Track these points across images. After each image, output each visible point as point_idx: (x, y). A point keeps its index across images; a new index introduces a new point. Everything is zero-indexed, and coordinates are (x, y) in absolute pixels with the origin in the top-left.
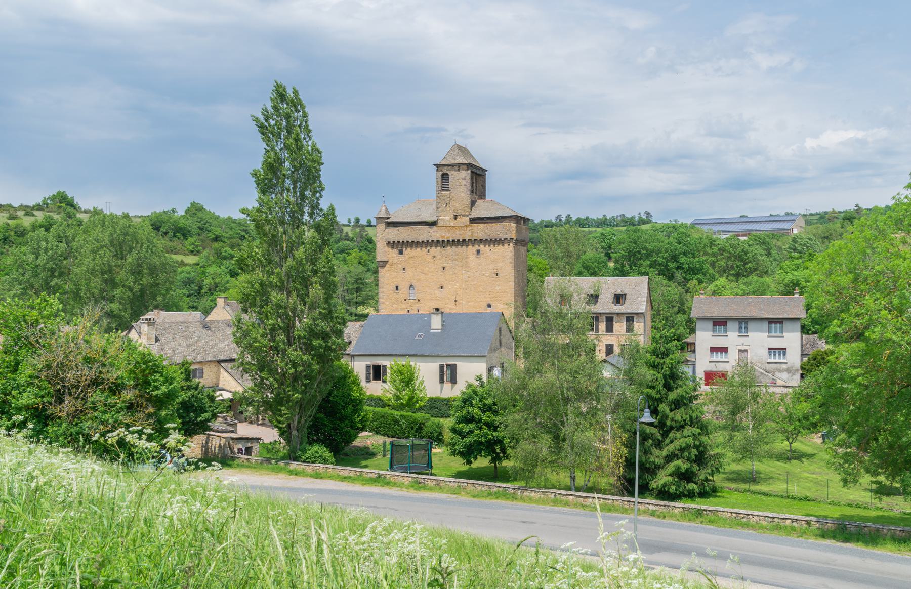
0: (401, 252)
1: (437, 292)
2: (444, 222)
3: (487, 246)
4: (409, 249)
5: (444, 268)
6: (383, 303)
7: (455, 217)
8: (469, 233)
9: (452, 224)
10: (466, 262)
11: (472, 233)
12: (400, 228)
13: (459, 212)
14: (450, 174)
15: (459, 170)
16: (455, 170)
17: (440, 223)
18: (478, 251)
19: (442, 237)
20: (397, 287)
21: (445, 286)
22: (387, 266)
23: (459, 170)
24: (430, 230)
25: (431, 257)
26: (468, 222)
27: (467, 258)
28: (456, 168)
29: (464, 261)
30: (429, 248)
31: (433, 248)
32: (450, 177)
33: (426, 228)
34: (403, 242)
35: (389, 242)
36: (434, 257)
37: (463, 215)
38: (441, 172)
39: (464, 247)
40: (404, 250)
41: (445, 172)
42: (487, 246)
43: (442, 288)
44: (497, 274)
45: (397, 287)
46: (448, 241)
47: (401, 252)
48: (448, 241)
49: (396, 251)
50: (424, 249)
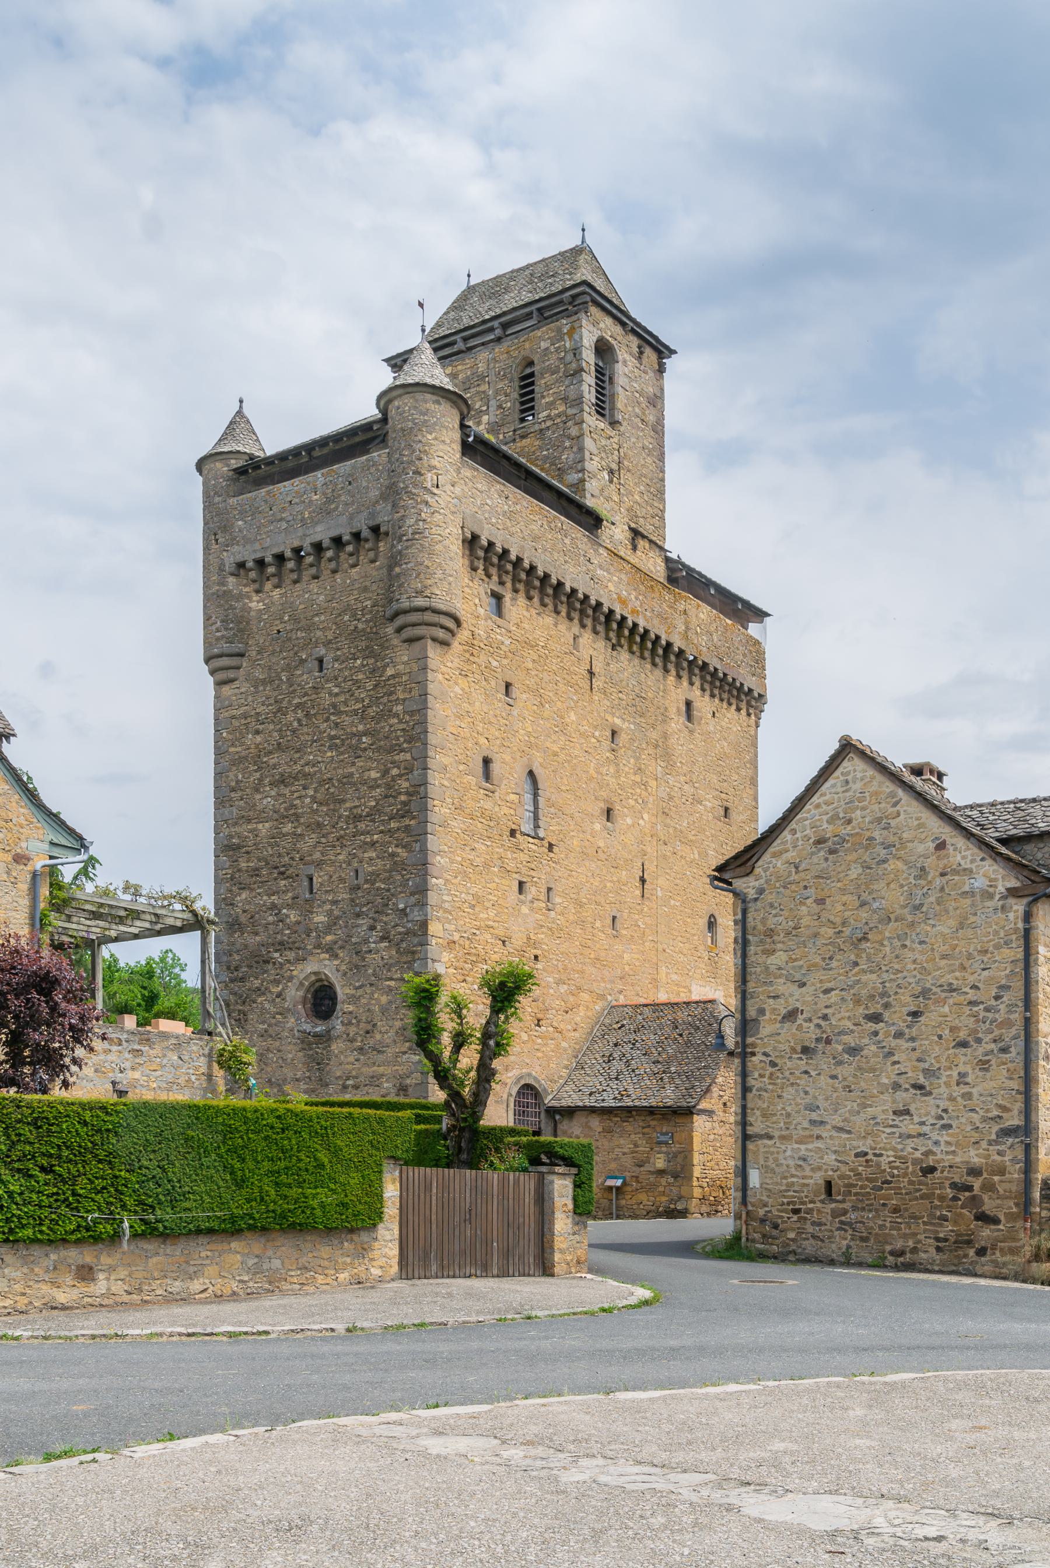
35: (475, 537)
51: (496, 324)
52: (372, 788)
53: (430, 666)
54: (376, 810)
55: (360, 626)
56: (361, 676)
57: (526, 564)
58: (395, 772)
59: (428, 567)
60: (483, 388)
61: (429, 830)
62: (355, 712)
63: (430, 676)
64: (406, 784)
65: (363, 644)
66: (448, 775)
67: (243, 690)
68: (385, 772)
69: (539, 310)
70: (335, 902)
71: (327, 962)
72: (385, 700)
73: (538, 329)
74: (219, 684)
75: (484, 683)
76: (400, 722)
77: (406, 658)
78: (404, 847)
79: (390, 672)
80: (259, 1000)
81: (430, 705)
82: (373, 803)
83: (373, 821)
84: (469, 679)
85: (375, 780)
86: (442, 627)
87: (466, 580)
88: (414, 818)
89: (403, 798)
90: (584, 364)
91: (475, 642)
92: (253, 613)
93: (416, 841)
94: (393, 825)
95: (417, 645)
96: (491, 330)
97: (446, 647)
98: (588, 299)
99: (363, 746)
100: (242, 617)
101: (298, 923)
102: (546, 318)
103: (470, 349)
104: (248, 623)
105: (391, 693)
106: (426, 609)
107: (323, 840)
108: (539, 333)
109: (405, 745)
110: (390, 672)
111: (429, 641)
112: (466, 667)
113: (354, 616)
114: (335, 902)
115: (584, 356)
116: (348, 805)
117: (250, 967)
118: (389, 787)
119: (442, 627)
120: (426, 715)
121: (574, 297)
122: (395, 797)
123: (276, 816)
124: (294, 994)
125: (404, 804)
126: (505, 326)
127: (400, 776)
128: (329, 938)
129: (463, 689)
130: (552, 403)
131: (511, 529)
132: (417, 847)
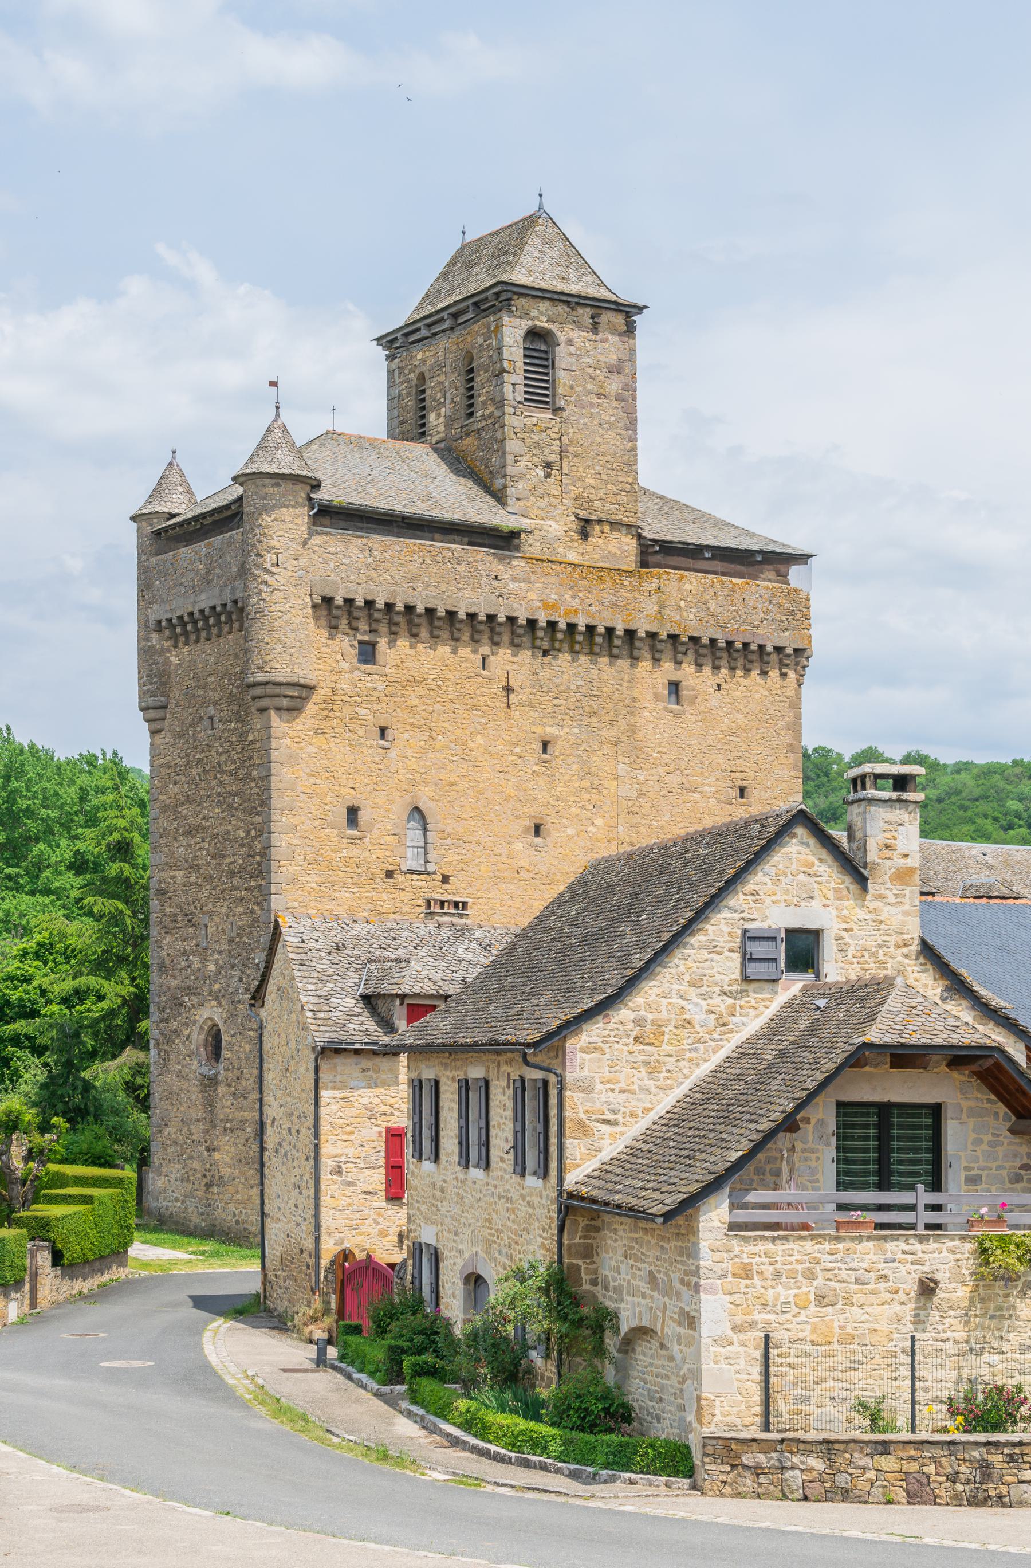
0: (368, 653)
1: (519, 846)
2: (543, 540)
3: (707, 671)
4: (403, 643)
5: (545, 745)
6: (292, 882)
7: (585, 528)
8: (650, 607)
9: (573, 557)
10: (632, 729)
11: (662, 606)
12: (378, 541)
13: (601, 509)
14: (561, 337)
15: (595, 328)
16: (578, 325)
17: (531, 546)
18: (675, 687)
19: (547, 606)
20: (353, 813)
21: (550, 821)
22: (310, 708)
23: (595, 328)
24: (500, 569)
25: (496, 688)
26: (630, 562)
27: (633, 709)
28: (585, 314)
29: (623, 723)
30: (485, 650)
31: (504, 653)
32: (562, 352)
33: (483, 558)
34: (389, 607)
35: (328, 600)
36: (508, 690)
37: (614, 525)
38: (526, 324)
39: (623, 663)
40: (383, 643)
41: (543, 323)
42: (707, 671)
43: (538, 830)
44: (742, 791)
45: (353, 813)
46: (572, 627)
47: (368, 653)
48: (572, 627)
49: (346, 645)
50: (465, 652)
51: (445, 314)
52: (241, 846)
53: (273, 735)
54: (243, 868)
55: (234, 691)
56: (234, 739)
57: (400, 607)
58: (253, 833)
59: (268, 644)
60: (442, 378)
61: (273, 890)
62: (231, 773)
63: (274, 744)
64: (259, 846)
65: (235, 708)
66: (298, 834)
67: (167, 740)
68: (248, 833)
69: (475, 304)
70: (220, 952)
71: (215, 1009)
72: (247, 763)
73: (475, 323)
74: (154, 732)
75: (349, 734)
76: (256, 786)
77: (259, 726)
78: (258, 905)
79: (250, 738)
80: (177, 1041)
81: (273, 772)
82: (241, 861)
83: (241, 877)
84: (327, 736)
85: (242, 839)
86: (285, 696)
87: (324, 640)
88: (264, 878)
89: (258, 858)
90: (506, 365)
91: (335, 698)
92: (172, 667)
93: (265, 900)
94: (253, 883)
95: (266, 714)
96: (443, 320)
97: (295, 713)
98: (509, 295)
99: (236, 805)
100: (164, 670)
101: (199, 969)
102: (484, 310)
103: (435, 334)
104: (169, 676)
105: (250, 758)
106: (267, 683)
107: (213, 892)
108: (475, 327)
109: (259, 809)
110: (250, 738)
111: (272, 712)
112: (322, 725)
113: (230, 680)
114: (220, 952)
115: (506, 355)
116: (228, 860)
117: (171, 1009)
118: (250, 848)
119: (285, 696)
120: (269, 782)
121: (498, 295)
122: (253, 857)
123: (186, 865)
124: (198, 1038)
125: (259, 864)
126: (455, 316)
127: (256, 837)
128: (217, 986)
129: (319, 747)
130: (484, 403)
131: (377, 579)
132: (266, 904)
